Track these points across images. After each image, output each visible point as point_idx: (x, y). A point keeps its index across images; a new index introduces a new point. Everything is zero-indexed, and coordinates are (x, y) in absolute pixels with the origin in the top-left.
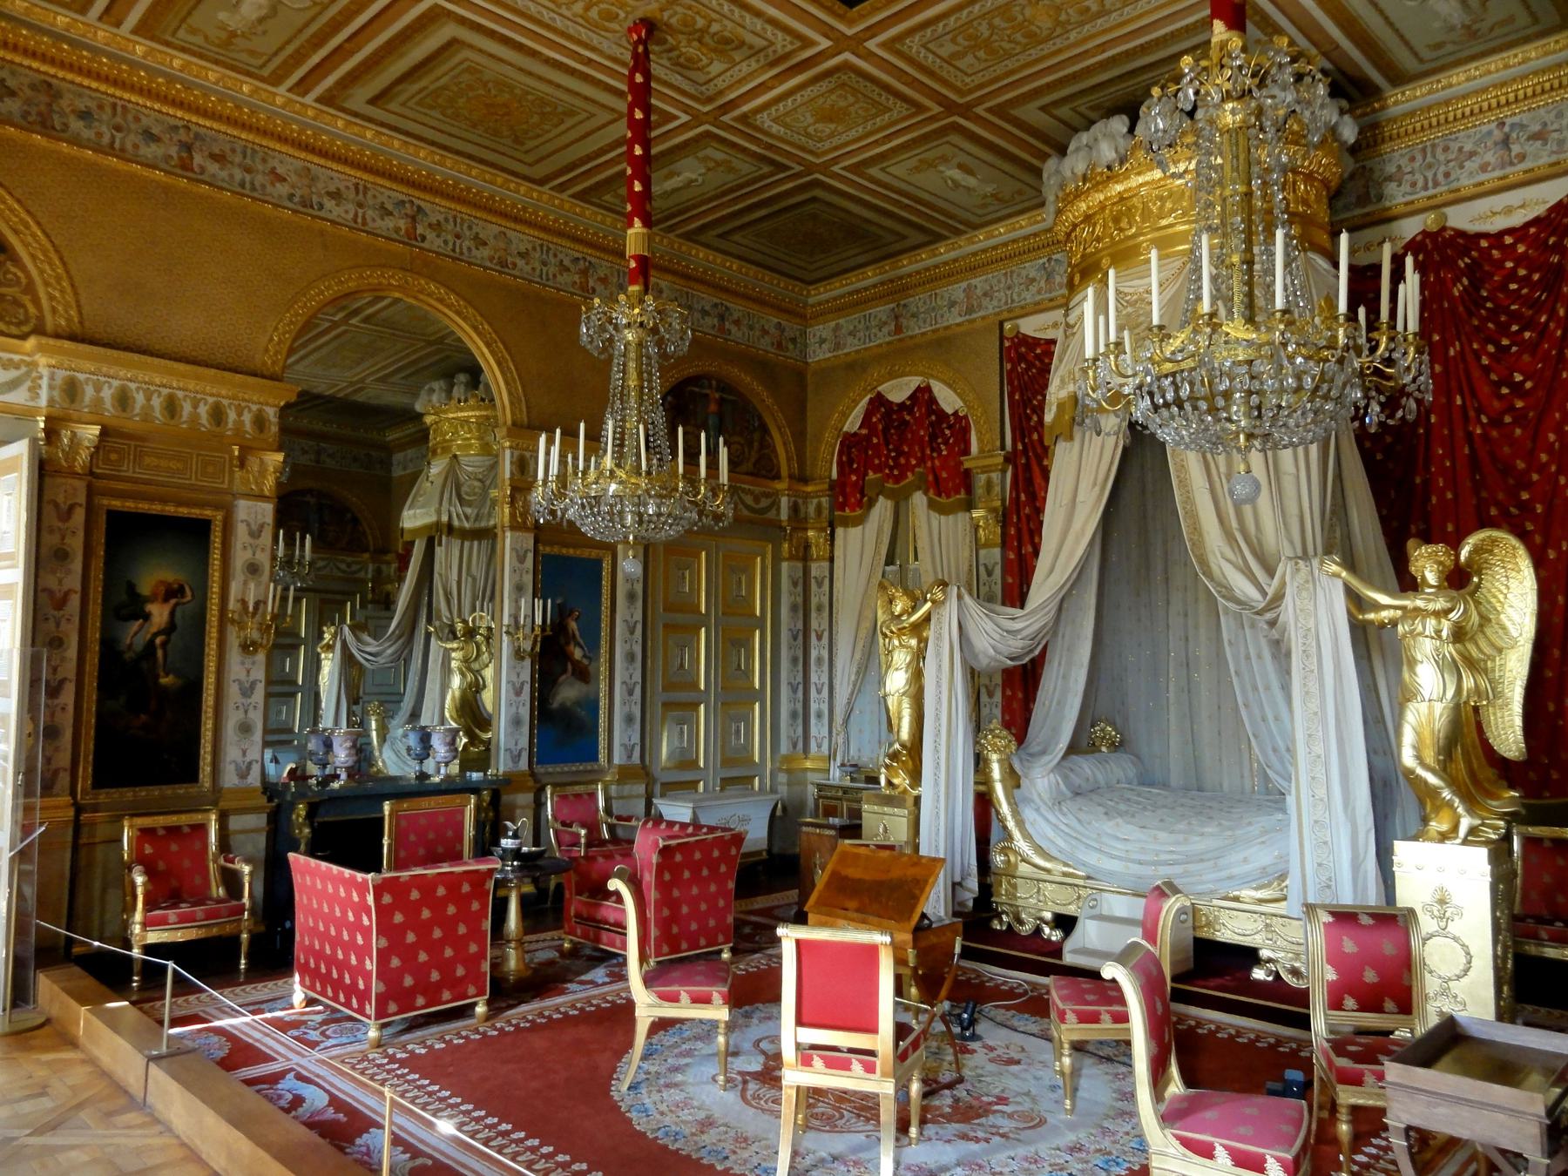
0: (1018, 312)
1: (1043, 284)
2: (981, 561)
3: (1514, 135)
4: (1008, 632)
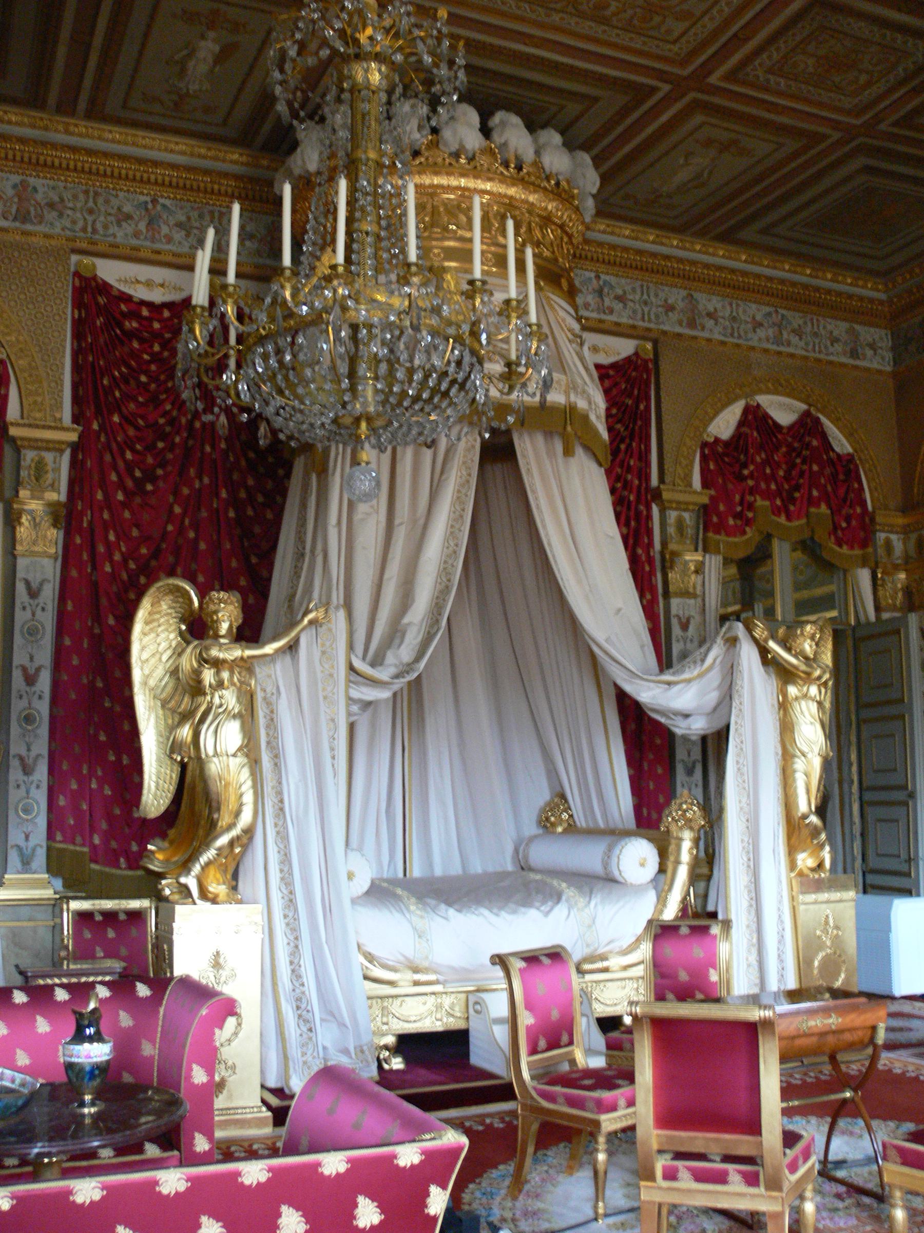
0: (101, 248)
1: (142, 226)
2: (20, 574)
3: (606, 290)
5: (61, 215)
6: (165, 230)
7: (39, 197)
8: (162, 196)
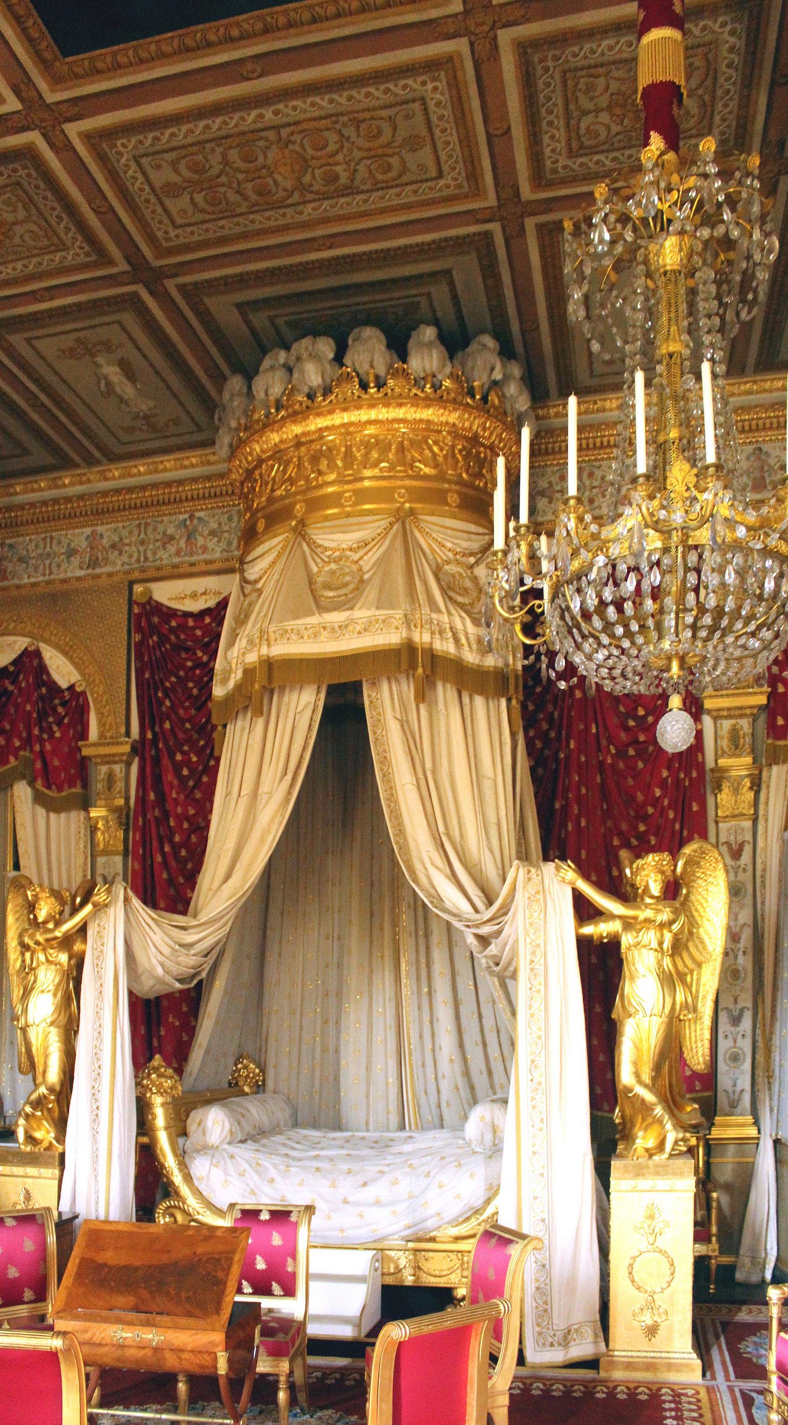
0: (150, 574)
1: (182, 543)
4: (181, 945)
5: (120, 554)
6: (200, 541)
7: (105, 542)
8: (197, 510)
